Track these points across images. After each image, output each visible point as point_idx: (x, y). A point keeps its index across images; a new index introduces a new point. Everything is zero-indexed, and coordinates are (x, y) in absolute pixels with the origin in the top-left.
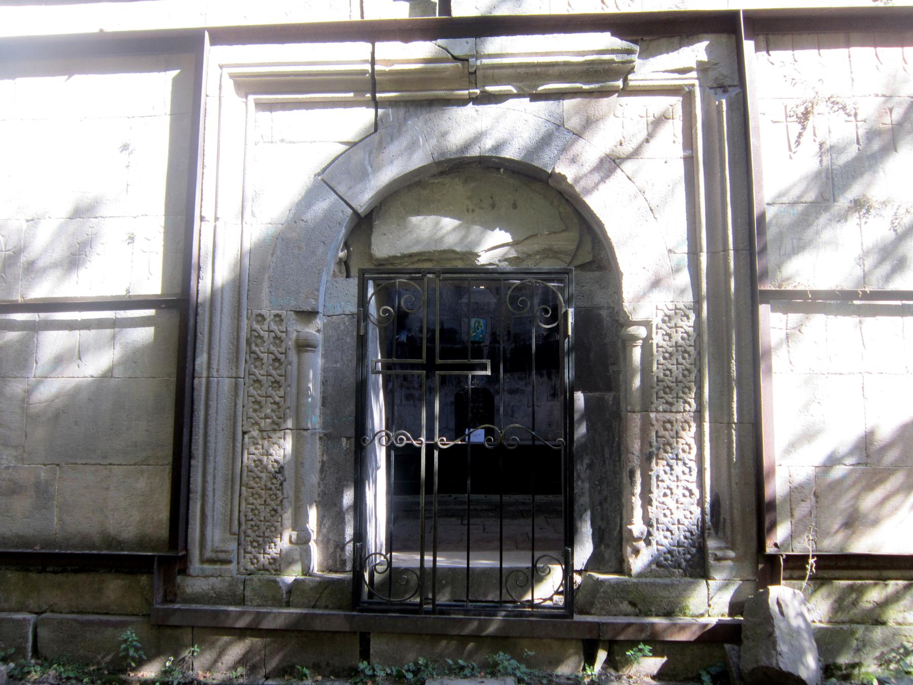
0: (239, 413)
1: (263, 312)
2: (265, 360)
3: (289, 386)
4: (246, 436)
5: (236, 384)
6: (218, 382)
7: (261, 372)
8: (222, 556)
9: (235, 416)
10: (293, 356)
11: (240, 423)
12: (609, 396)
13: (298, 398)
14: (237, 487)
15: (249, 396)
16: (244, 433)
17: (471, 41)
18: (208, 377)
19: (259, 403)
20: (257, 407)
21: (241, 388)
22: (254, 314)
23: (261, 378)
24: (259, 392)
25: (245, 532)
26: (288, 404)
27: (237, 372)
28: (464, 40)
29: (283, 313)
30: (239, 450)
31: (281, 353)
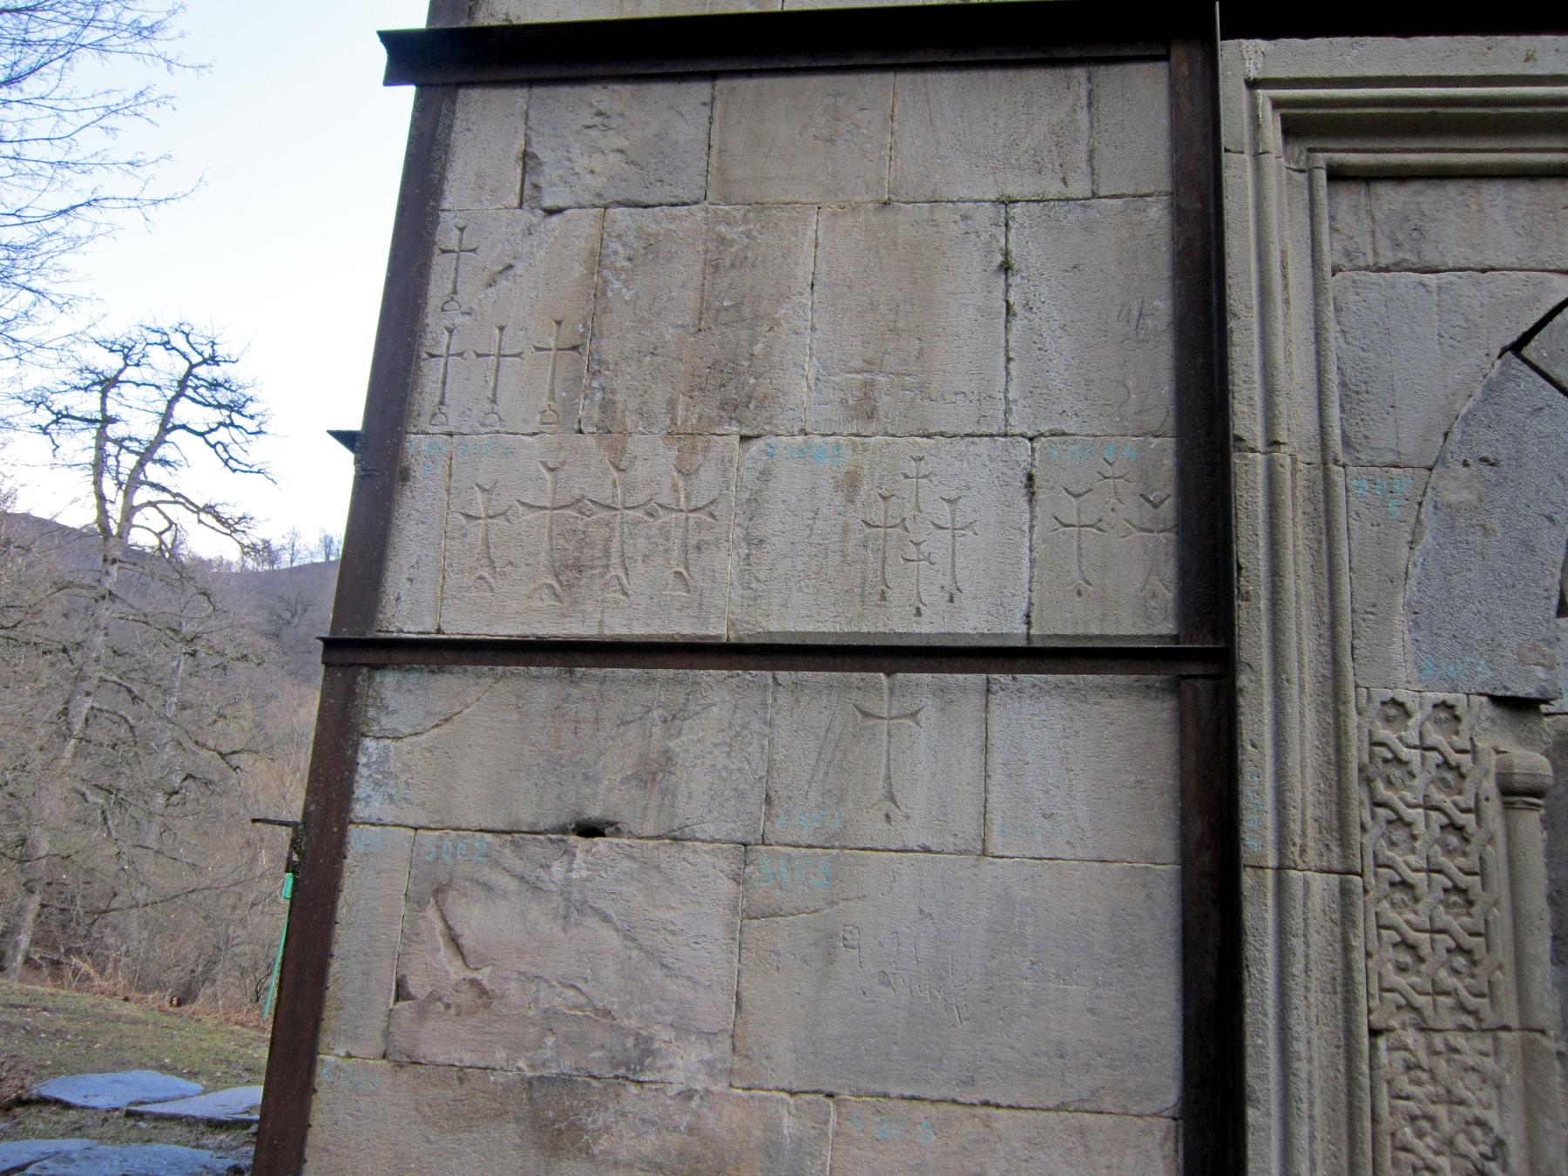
0: (1360, 977)
1: (1403, 695)
2: (1420, 828)
3: (1496, 903)
4: (1382, 1042)
5: (1345, 892)
6: (1306, 883)
15: (1380, 927)
16: (1374, 1033)
18: (1281, 869)
19: (1412, 947)
23: (1413, 877)
24: (1411, 917)
27: (1345, 857)
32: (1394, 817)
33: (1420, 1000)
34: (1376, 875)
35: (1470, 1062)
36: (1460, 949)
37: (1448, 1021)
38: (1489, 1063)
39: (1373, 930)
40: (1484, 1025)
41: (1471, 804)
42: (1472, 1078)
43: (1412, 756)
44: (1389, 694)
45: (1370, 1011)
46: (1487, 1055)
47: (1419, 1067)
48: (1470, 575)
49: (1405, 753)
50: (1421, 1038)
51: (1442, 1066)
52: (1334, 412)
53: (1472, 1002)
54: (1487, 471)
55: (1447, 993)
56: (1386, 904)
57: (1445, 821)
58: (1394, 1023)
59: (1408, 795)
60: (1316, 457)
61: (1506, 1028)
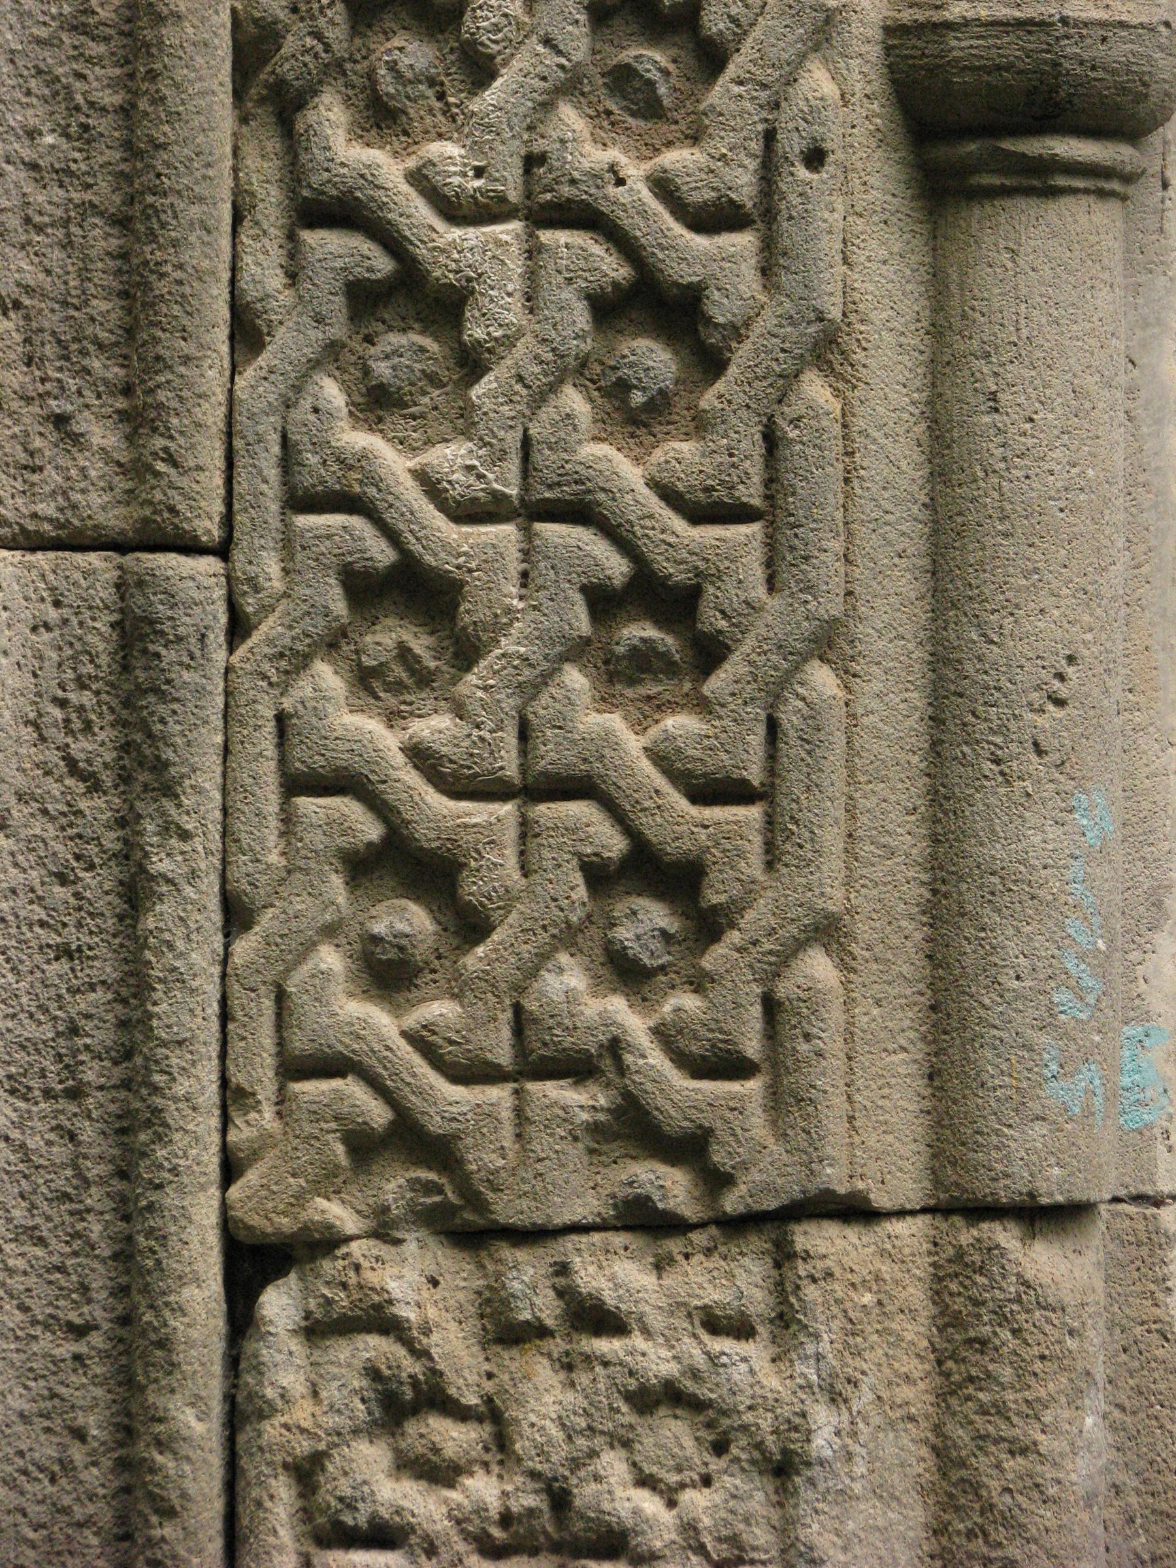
0: (187, 1013)
2: (498, 310)
3: (827, 642)
4: (279, 1304)
5: (137, 628)
7: (451, 457)
9: (135, 1046)
10: (858, 232)
11: (196, 1142)
13: (943, 810)
15: (295, 784)
16: (252, 1262)
20: (409, 920)
21: (201, 677)
23: (447, 541)
24: (435, 727)
30: (198, 1479)
31: (715, 218)
32: (383, 265)
33: (448, 1101)
34: (288, 544)
35: (657, 1361)
36: (651, 869)
37: (578, 1191)
38: (749, 1369)
39: (269, 796)
40: (732, 1203)
41: (742, 182)
42: (674, 1435)
45: (230, 1170)
46: (742, 1330)
47: (434, 1398)
50: (461, 1275)
51: (545, 1400)
53: (678, 1093)
55: (576, 1068)
56: (327, 677)
57: (612, 268)
58: (339, 1213)
59: (447, 153)
61: (856, 1211)
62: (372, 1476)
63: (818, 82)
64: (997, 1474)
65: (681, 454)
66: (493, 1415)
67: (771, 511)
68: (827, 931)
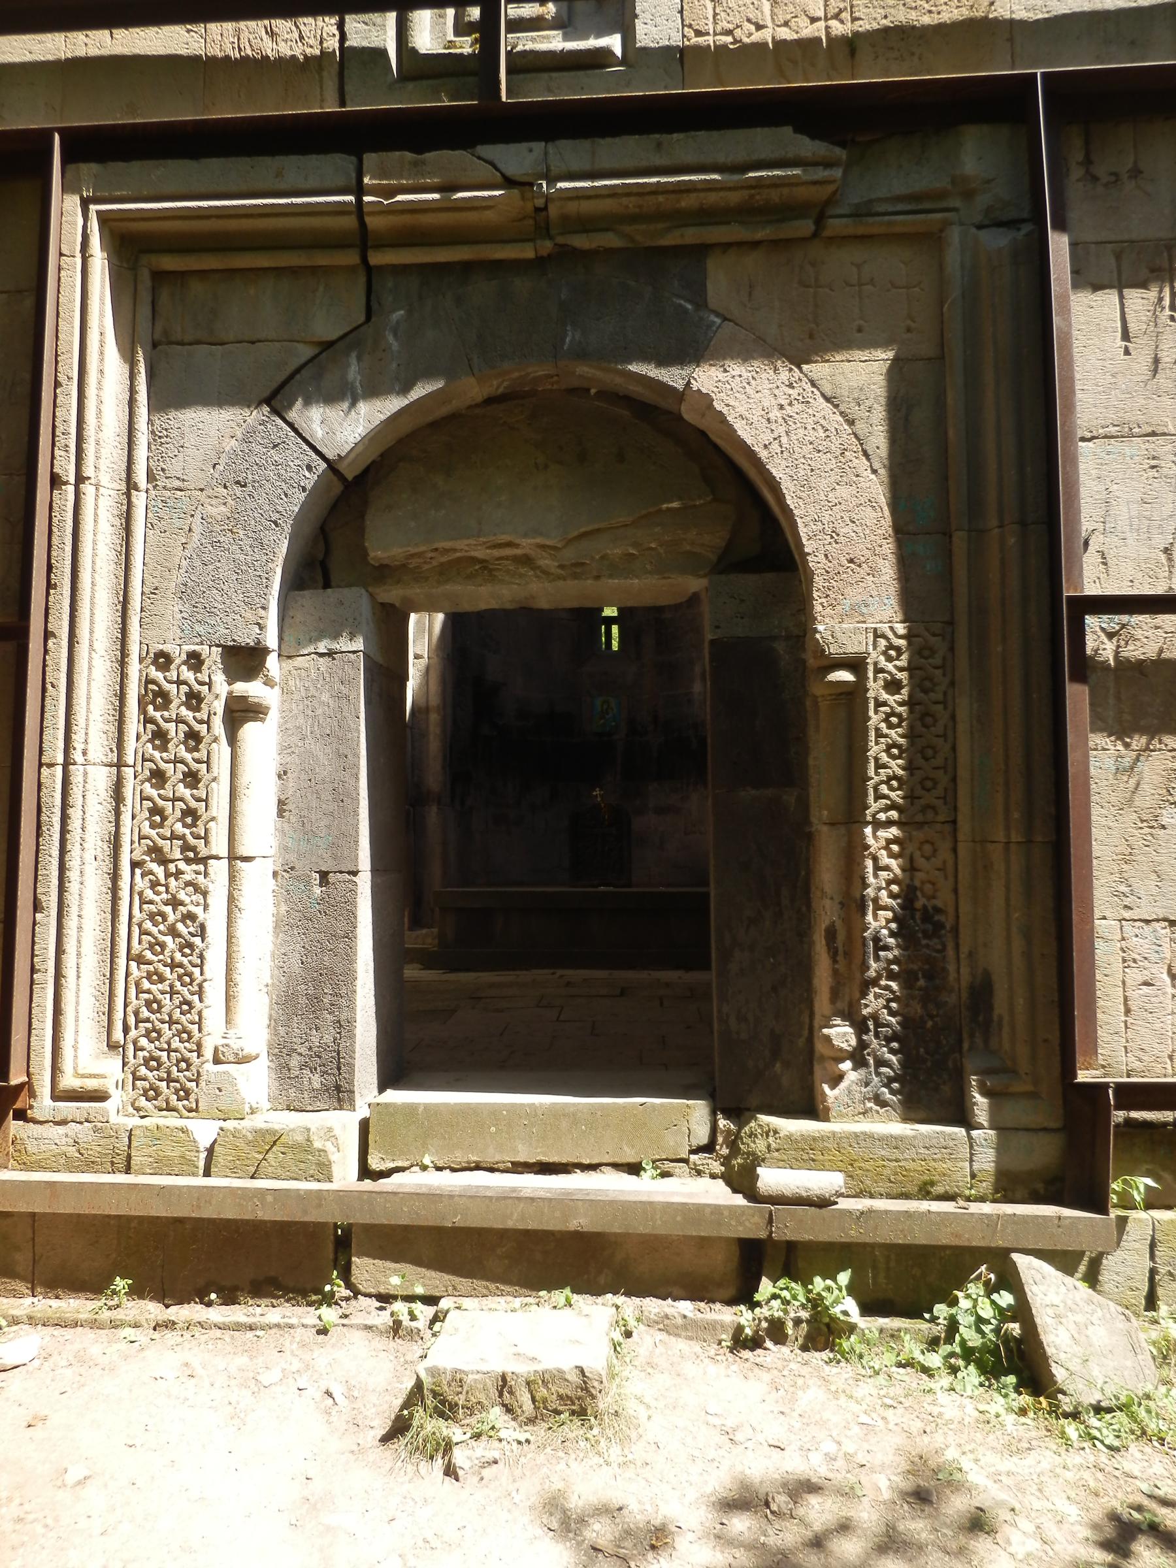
0: (126, 830)
1: (167, 648)
2: (172, 733)
4: (138, 871)
6: (86, 774)
8: (91, 1084)
12: (790, 798)
14: (122, 961)
16: (134, 865)
17: (538, 147)
22: (152, 651)
25: (135, 1043)
26: (213, 812)
28: (524, 146)
29: (204, 650)
33: (160, 842)
35: (187, 877)
43: (173, 688)
44: (161, 647)
48: (219, 565)
49: (167, 686)
52: (141, 453)
54: (238, 490)
55: (178, 838)
60: (124, 487)
61: (217, 858)
62: (149, 894)
63: (216, 703)
64: (236, 893)
65: (196, 755)
66: (167, 886)
67: (208, 762)
68: (213, 819)
